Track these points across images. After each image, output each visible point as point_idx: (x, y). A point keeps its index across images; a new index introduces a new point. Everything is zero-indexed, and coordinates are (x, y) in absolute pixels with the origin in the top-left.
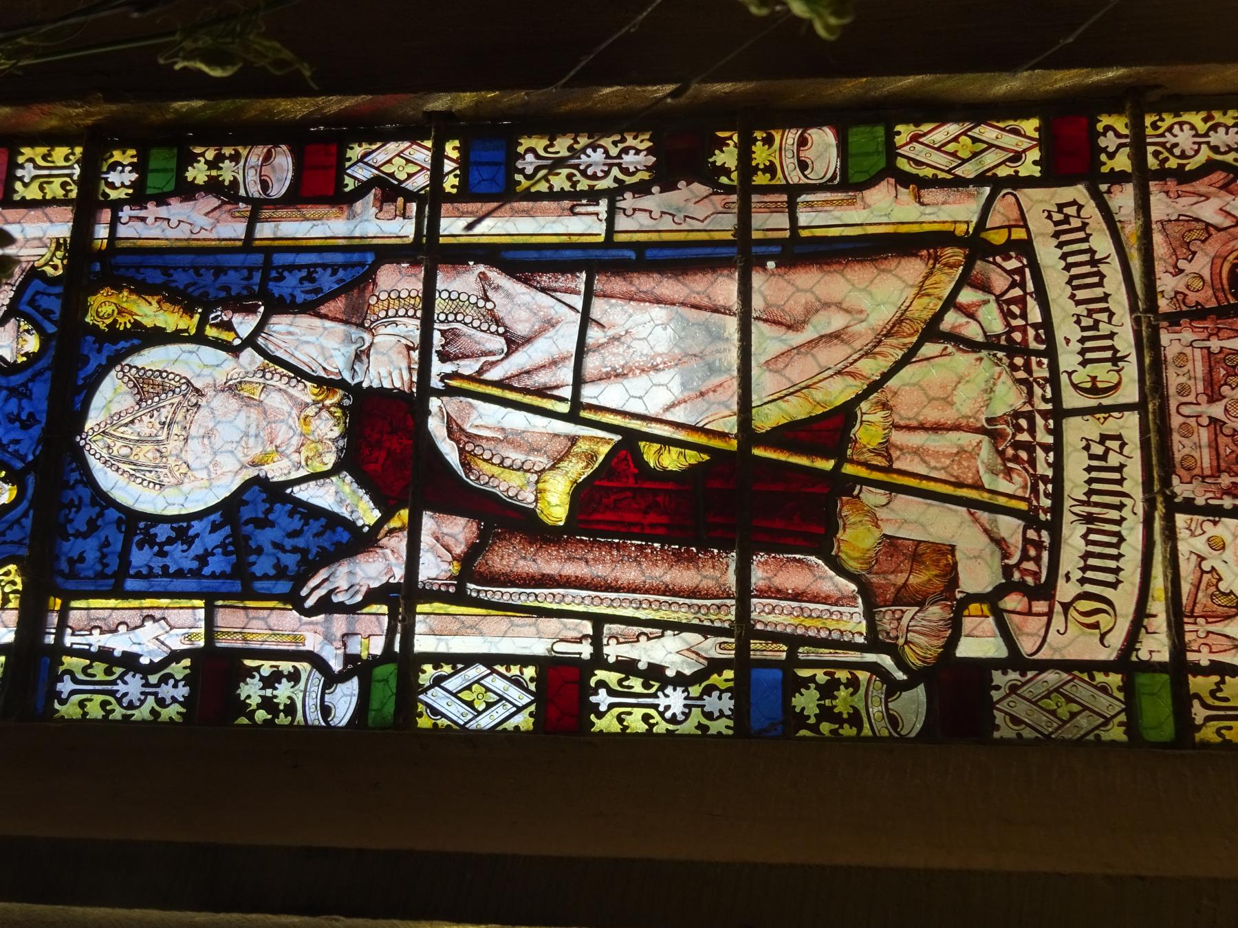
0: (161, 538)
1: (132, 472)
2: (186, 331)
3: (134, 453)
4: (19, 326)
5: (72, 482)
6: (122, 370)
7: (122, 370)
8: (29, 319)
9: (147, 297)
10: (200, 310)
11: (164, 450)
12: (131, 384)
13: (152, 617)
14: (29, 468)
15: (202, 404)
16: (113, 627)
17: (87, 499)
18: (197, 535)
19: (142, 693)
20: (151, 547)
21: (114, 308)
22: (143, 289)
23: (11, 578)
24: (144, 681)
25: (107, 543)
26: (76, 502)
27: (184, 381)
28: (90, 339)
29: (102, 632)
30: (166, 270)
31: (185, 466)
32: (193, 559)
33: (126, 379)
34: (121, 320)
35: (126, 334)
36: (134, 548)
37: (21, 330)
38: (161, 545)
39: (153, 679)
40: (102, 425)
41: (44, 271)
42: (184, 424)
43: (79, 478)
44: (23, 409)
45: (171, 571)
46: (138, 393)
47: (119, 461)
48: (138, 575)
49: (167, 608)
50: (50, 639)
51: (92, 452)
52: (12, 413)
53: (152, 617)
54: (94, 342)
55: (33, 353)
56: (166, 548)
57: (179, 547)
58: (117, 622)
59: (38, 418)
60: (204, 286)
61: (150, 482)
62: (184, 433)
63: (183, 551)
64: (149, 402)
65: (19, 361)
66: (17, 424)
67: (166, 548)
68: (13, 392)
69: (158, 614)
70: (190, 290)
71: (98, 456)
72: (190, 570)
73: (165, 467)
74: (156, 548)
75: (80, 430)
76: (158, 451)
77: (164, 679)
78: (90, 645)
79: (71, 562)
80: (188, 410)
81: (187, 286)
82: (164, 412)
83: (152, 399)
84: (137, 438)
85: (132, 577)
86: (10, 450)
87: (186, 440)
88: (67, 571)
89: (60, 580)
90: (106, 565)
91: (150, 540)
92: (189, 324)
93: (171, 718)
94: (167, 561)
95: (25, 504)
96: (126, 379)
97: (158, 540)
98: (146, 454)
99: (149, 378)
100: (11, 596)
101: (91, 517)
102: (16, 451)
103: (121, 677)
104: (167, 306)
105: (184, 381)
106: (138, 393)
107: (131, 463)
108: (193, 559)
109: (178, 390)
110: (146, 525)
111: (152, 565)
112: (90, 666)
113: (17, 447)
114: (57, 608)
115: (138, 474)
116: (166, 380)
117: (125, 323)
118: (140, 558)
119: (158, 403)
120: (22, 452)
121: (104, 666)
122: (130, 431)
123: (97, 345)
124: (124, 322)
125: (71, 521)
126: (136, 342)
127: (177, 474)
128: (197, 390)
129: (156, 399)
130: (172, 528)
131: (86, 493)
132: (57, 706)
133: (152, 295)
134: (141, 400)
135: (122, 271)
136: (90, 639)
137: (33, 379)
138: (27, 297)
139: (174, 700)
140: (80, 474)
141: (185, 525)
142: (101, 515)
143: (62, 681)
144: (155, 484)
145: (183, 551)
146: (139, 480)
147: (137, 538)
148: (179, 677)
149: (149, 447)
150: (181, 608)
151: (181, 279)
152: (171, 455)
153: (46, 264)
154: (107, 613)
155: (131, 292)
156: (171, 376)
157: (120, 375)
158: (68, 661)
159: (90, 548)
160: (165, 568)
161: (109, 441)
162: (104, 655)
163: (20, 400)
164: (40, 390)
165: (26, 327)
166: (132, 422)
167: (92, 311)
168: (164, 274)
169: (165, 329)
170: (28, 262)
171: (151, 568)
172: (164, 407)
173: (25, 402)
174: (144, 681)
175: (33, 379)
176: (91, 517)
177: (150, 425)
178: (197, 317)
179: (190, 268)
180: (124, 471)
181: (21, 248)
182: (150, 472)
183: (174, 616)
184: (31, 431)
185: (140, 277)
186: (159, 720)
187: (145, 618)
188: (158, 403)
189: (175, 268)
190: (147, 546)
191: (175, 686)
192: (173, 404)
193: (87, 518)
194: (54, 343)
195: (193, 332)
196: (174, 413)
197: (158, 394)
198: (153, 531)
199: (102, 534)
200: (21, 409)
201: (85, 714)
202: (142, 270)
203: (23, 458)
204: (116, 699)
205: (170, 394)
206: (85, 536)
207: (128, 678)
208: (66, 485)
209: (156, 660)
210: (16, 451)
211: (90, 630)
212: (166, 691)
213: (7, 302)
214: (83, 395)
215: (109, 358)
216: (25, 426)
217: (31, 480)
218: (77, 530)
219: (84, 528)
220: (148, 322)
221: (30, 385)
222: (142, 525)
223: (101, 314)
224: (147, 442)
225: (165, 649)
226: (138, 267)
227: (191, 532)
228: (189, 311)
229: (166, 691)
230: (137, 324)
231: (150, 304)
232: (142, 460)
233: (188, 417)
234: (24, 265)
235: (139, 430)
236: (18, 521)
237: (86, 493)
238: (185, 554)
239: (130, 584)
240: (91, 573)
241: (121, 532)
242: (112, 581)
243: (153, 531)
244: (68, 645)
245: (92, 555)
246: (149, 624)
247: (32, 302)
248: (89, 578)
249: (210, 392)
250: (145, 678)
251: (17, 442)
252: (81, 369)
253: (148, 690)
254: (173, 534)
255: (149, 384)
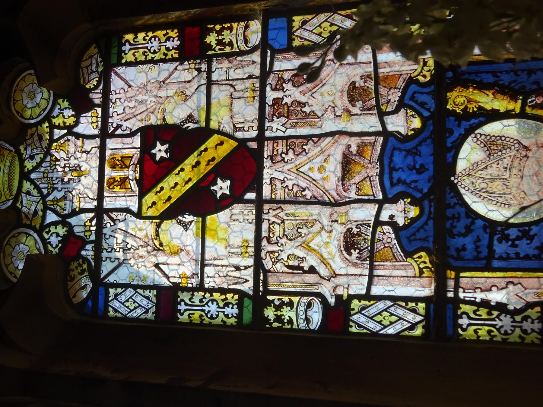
0: (513, 237)
1: (489, 198)
2: (513, 110)
3: (490, 186)
4: (407, 113)
5: (452, 204)
6: (476, 137)
7: (476, 137)
8: (413, 109)
9: (485, 91)
10: (521, 98)
11: (508, 184)
12: (482, 145)
13: (512, 283)
14: (426, 196)
15: (530, 156)
16: (488, 288)
17: (463, 215)
18: (536, 235)
19: (512, 326)
20: (507, 242)
21: (465, 99)
22: (482, 87)
23: (423, 259)
24: (512, 320)
25: (478, 240)
26: (457, 216)
27: (516, 142)
28: (452, 119)
29: (482, 291)
30: (494, 74)
31: (523, 193)
32: (535, 249)
33: (479, 142)
34: (470, 106)
35: (474, 115)
36: (495, 242)
37: (408, 115)
38: (513, 240)
39: (518, 318)
40: (467, 170)
41: (417, 79)
42: (519, 168)
43: (456, 201)
44: (416, 162)
45: (521, 255)
46: (488, 150)
47: (480, 191)
48: (501, 258)
49: (521, 277)
50: (450, 295)
51: (463, 186)
52: (410, 165)
53: (512, 283)
54: (455, 121)
55: (418, 129)
56: (517, 242)
57: (525, 241)
58: (490, 285)
59: (427, 167)
60: (522, 82)
61: (502, 203)
62: (520, 173)
63: (528, 244)
64: (495, 155)
65: (409, 134)
66: (414, 171)
67: (517, 242)
68: (409, 152)
69: (516, 281)
70: (512, 85)
71: (466, 188)
72: (534, 255)
73: (510, 194)
74: (510, 243)
75: (454, 173)
76: (505, 185)
77: (525, 318)
78: (475, 298)
79: (458, 250)
80: (521, 160)
81: (510, 83)
82: (505, 161)
83: (497, 153)
84: (490, 177)
85: (497, 259)
86: (412, 186)
87: (522, 177)
88: (456, 255)
89: (451, 261)
90: (479, 252)
91: (505, 238)
92: (516, 106)
93: (532, 341)
94: (517, 250)
95: (424, 218)
96: (479, 142)
97: (511, 238)
98: (497, 187)
99: (493, 141)
100: (424, 270)
101: (467, 225)
102: (416, 187)
103: (498, 317)
104: (499, 96)
105: (516, 142)
106: (488, 150)
107: (488, 192)
108: (535, 249)
109: (513, 148)
110: (502, 229)
111: (508, 252)
112: (478, 310)
113: (416, 184)
114: (453, 276)
115: (493, 199)
116: (505, 142)
117: (473, 108)
118: (500, 248)
119: (501, 155)
120: (420, 187)
121: (486, 310)
122: (485, 173)
123: (457, 122)
124: (472, 107)
125: (455, 227)
126: (482, 119)
127: (519, 198)
128: (526, 147)
129: (500, 153)
130: (519, 231)
131: (462, 210)
132: (460, 332)
133: (488, 89)
134: (490, 154)
135: (466, 76)
136: (475, 295)
137: (420, 144)
138: (407, 96)
139: (533, 330)
140: (457, 200)
141: (527, 228)
142: (473, 223)
143: (462, 318)
144: (505, 204)
145: (528, 244)
146: (495, 203)
147: (496, 237)
148: (534, 317)
149: (498, 182)
150: (530, 277)
151: (506, 79)
152: (513, 187)
153: (419, 75)
154: (483, 279)
155: (475, 88)
156: (508, 139)
157: (475, 140)
158: (465, 308)
159: (468, 241)
160: (517, 254)
161: (473, 180)
162: (485, 303)
163: (414, 157)
164: (426, 150)
165: (411, 114)
166: (486, 168)
167: (450, 102)
168: (494, 76)
169: (499, 110)
170: (407, 74)
171: (508, 254)
172: (505, 158)
173: (417, 158)
174: (512, 320)
175: (420, 144)
176: (467, 225)
177: (498, 169)
178: (520, 102)
179: (511, 71)
180: (485, 197)
181: (401, 66)
182: (501, 197)
183: (525, 282)
184: (423, 175)
185: (478, 79)
186: (525, 342)
187: (508, 283)
188: (501, 155)
189: (501, 72)
190: (504, 242)
191: (533, 322)
192: (510, 156)
193: (465, 225)
194: (431, 122)
195: (518, 111)
196: (512, 161)
197: (500, 151)
198: (506, 232)
199: (474, 234)
200: (415, 162)
201: (478, 337)
202: (479, 75)
203: (421, 191)
204: (496, 329)
205: (508, 150)
206: (465, 235)
207: (502, 317)
208: (449, 206)
209: (518, 307)
210: (416, 187)
211: (474, 290)
212: (527, 325)
213: (397, 99)
214: (452, 153)
215: (465, 129)
216: (419, 172)
217: (426, 203)
218: (459, 232)
219: (463, 231)
220: (488, 107)
221: (419, 147)
222: (499, 229)
223: (457, 103)
224: (497, 179)
225: (523, 301)
226: (477, 73)
227: (532, 233)
228: (514, 98)
229: (527, 325)
230: (480, 108)
231: (488, 95)
232: (495, 190)
233: (522, 163)
234: (405, 76)
235: (491, 172)
236: (422, 227)
237: (462, 210)
238: (528, 246)
239: (496, 264)
240: (470, 257)
241: (486, 233)
242: (484, 262)
243: (506, 232)
244: (462, 298)
245: (470, 247)
246: (511, 287)
247: (412, 98)
248: (470, 260)
249: (534, 148)
250: (512, 317)
251: (416, 181)
252: (449, 137)
253: (515, 324)
254: (520, 234)
255: (494, 145)
